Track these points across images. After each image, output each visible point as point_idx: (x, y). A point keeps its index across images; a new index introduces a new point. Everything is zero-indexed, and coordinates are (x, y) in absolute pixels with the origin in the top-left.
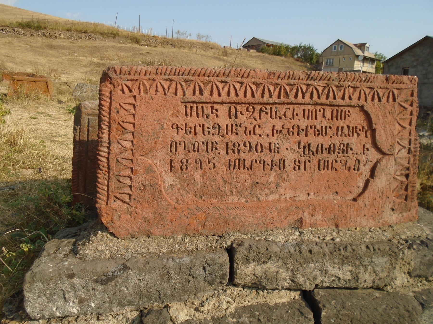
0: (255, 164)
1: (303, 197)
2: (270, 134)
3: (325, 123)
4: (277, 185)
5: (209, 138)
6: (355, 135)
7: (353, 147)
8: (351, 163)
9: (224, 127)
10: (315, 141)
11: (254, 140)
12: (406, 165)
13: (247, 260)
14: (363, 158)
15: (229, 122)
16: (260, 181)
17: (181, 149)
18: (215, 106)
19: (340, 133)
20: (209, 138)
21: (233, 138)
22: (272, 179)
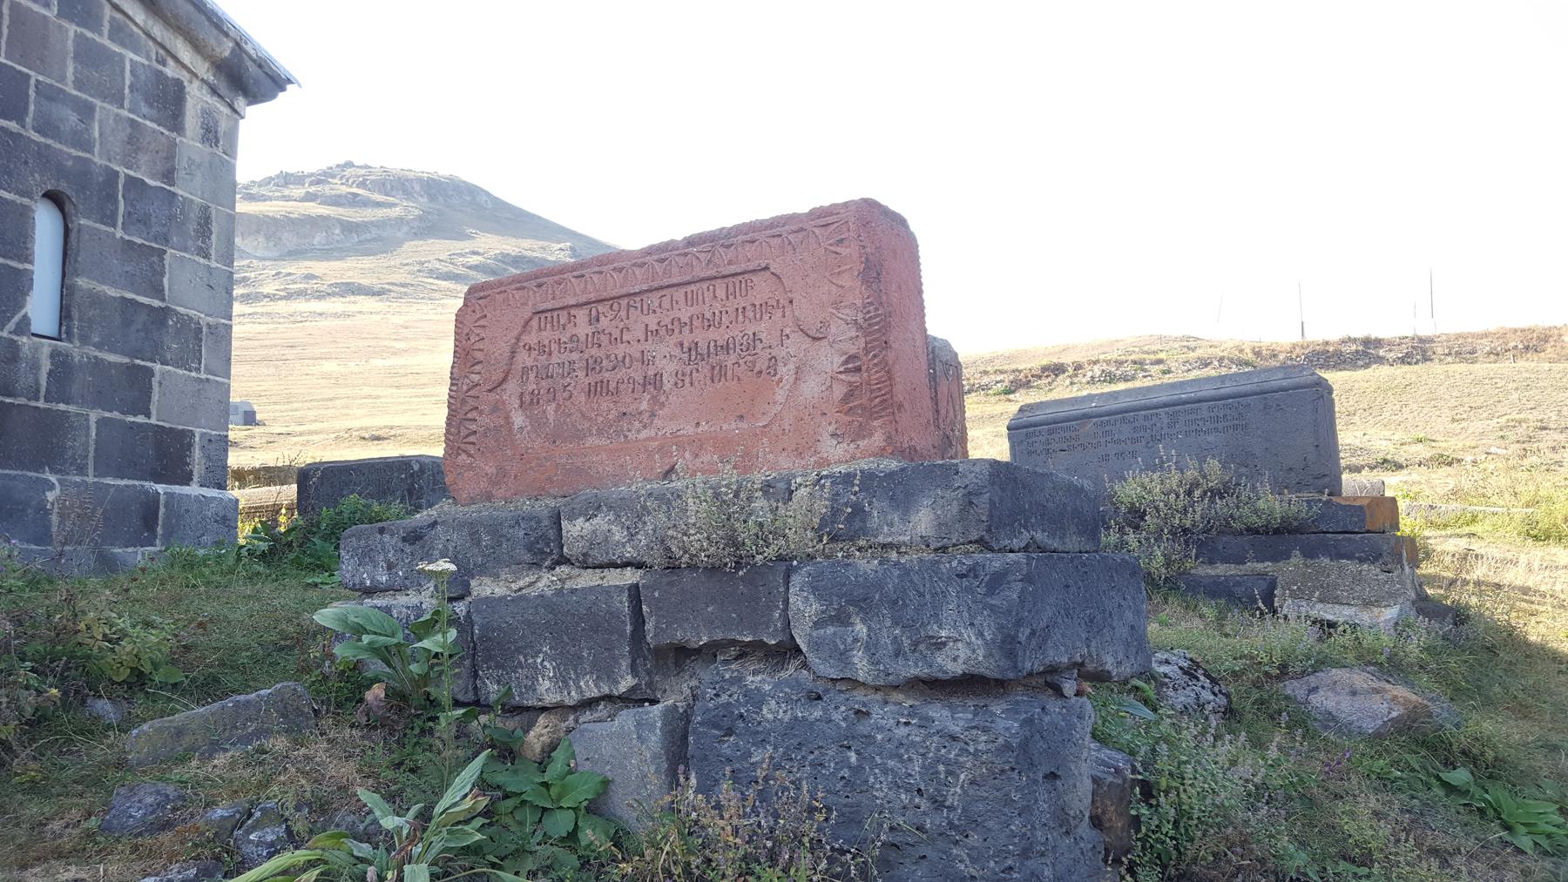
0: (622, 387)
1: (690, 430)
2: (642, 338)
3: (718, 307)
4: (653, 415)
5: (566, 357)
6: (766, 317)
7: (763, 336)
8: (762, 364)
9: (583, 339)
10: (702, 337)
11: (621, 350)
12: (853, 350)
13: (572, 518)
14: (779, 352)
15: (589, 330)
16: (628, 410)
17: (532, 376)
18: (573, 312)
19: (741, 318)
20: (566, 357)
21: (594, 351)
22: (644, 406)
